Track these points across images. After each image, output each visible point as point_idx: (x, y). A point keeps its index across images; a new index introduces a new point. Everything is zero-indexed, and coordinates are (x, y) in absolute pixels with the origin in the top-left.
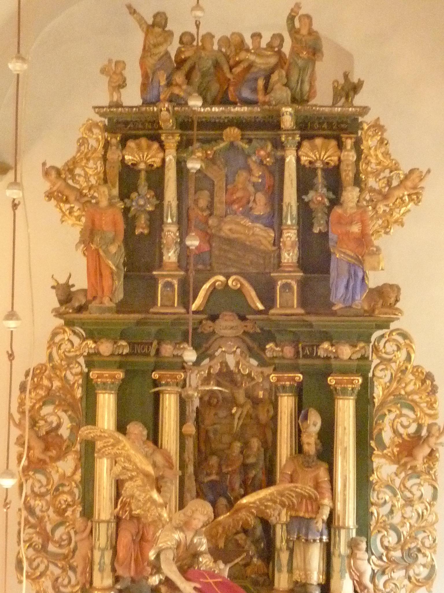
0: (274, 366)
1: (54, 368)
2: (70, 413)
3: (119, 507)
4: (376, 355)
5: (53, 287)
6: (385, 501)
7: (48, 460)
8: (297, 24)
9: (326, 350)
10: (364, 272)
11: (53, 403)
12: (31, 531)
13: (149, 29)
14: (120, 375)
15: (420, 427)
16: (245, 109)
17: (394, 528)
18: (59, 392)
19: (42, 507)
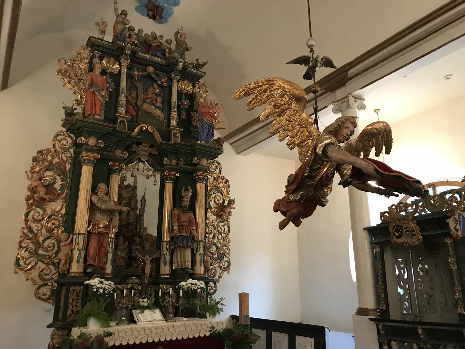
0: (161, 171)
1: (55, 151)
2: (61, 177)
3: (91, 226)
4: (209, 169)
5: (64, 108)
6: (212, 231)
7: (48, 199)
8: (179, 37)
9: (196, 160)
10: (213, 131)
11: (52, 170)
12: (29, 241)
13: (118, 16)
14: (99, 156)
15: (224, 201)
16: (159, 60)
17: (215, 245)
18: (57, 164)
19: (38, 227)
